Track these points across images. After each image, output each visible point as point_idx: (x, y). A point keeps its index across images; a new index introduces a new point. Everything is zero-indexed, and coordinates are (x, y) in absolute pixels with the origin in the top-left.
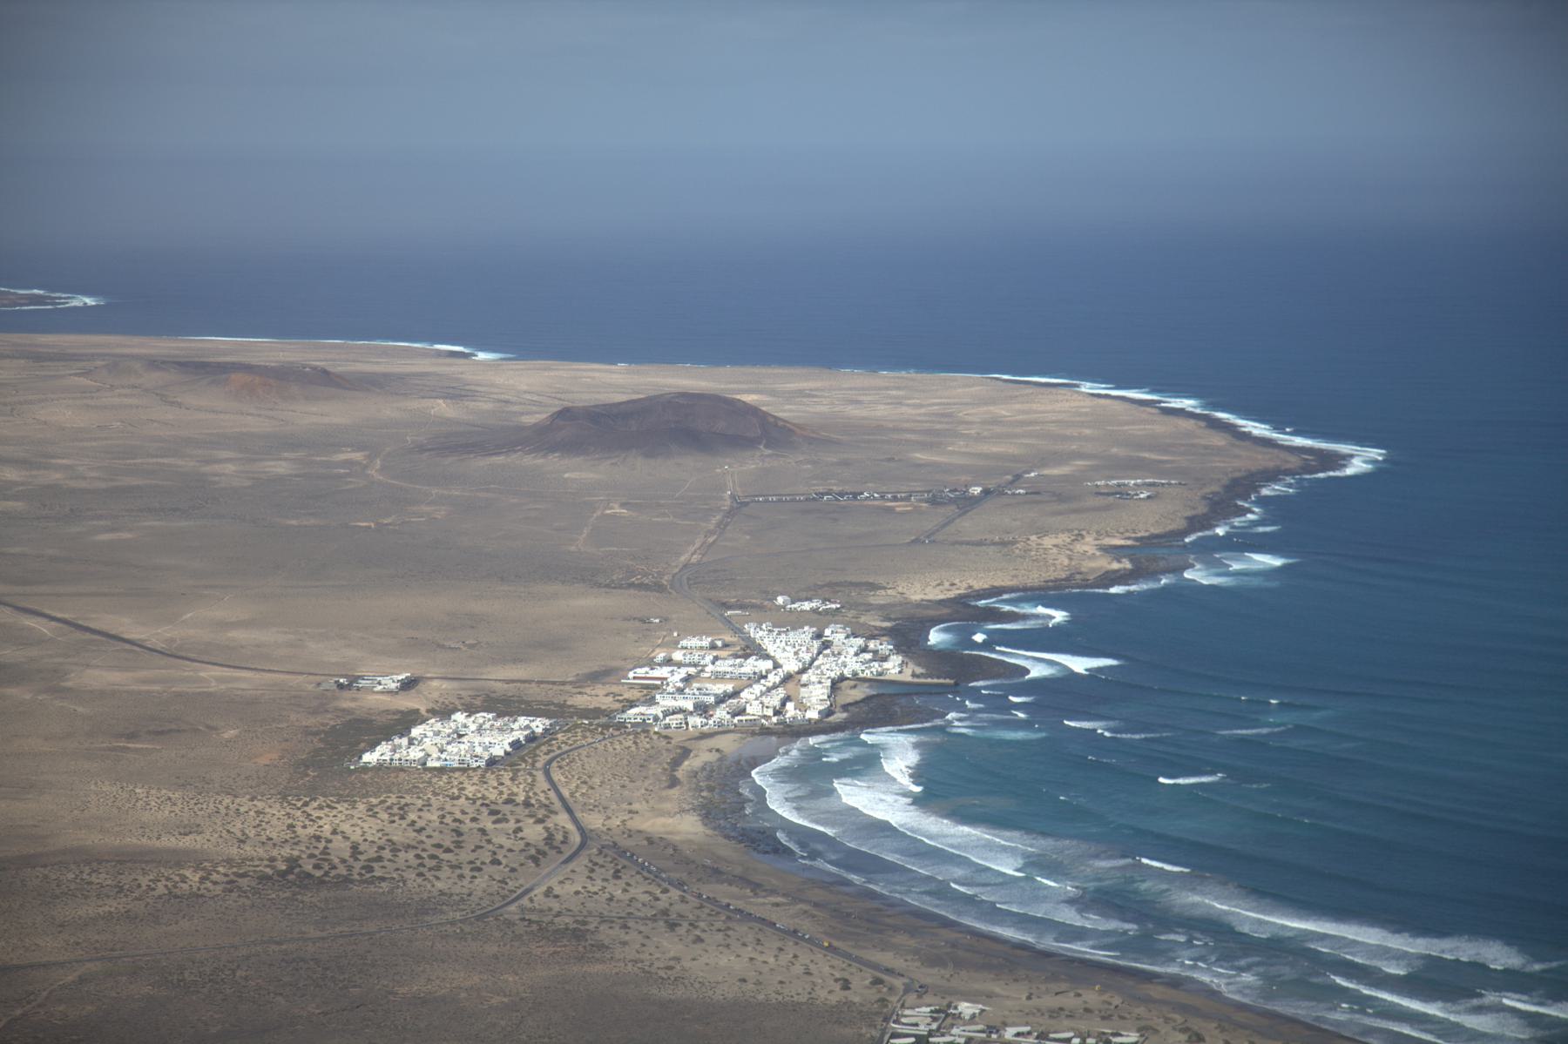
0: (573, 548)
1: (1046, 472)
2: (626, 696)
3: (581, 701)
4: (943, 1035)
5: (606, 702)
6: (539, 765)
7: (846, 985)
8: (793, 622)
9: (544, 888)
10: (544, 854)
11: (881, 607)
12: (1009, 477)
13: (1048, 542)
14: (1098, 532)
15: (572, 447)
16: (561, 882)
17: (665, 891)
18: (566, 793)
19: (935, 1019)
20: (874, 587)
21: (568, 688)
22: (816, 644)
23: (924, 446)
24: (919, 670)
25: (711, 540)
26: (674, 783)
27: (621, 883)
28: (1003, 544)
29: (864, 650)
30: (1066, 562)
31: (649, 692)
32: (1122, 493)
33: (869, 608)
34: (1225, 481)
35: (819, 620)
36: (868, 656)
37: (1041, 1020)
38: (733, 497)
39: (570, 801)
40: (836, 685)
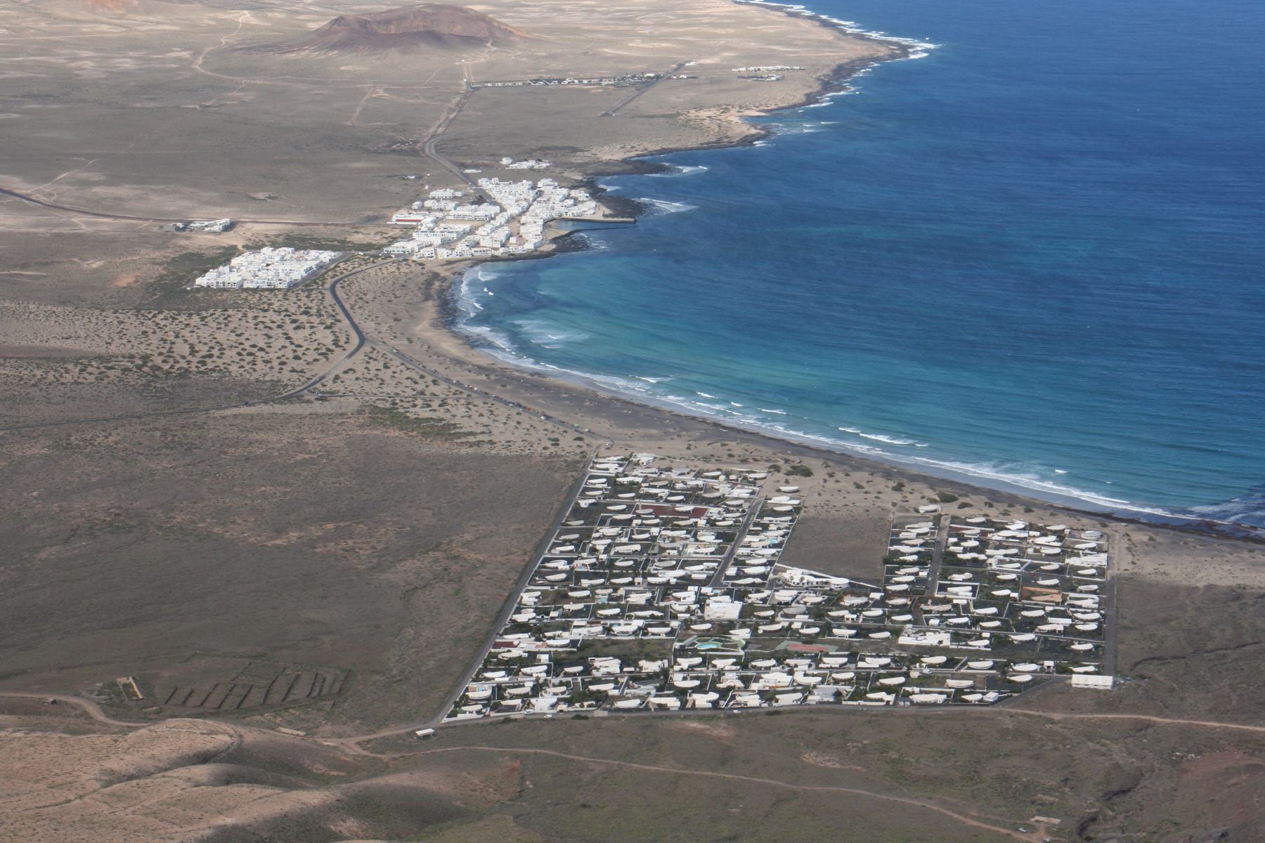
0: (349, 123)
1: (702, 61)
2: (391, 234)
3: (358, 238)
4: (626, 476)
5: (377, 239)
7: (556, 442)
9: (333, 376)
10: (332, 351)
13: (704, 114)
14: (741, 107)
16: (345, 372)
17: (422, 377)
18: (347, 307)
19: (621, 465)
20: (574, 150)
21: (347, 228)
22: (532, 193)
23: (609, 43)
24: (608, 211)
25: (452, 116)
26: (428, 297)
27: (389, 372)
28: (671, 116)
29: (568, 197)
30: (717, 129)
31: (407, 232)
32: (758, 78)
33: (570, 166)
34: (834, 66)
35: (534, 175)
36: (571, 202)
37: (696, 463)
38: (468, 83)
39: (351, 312)
40: (547, 224)
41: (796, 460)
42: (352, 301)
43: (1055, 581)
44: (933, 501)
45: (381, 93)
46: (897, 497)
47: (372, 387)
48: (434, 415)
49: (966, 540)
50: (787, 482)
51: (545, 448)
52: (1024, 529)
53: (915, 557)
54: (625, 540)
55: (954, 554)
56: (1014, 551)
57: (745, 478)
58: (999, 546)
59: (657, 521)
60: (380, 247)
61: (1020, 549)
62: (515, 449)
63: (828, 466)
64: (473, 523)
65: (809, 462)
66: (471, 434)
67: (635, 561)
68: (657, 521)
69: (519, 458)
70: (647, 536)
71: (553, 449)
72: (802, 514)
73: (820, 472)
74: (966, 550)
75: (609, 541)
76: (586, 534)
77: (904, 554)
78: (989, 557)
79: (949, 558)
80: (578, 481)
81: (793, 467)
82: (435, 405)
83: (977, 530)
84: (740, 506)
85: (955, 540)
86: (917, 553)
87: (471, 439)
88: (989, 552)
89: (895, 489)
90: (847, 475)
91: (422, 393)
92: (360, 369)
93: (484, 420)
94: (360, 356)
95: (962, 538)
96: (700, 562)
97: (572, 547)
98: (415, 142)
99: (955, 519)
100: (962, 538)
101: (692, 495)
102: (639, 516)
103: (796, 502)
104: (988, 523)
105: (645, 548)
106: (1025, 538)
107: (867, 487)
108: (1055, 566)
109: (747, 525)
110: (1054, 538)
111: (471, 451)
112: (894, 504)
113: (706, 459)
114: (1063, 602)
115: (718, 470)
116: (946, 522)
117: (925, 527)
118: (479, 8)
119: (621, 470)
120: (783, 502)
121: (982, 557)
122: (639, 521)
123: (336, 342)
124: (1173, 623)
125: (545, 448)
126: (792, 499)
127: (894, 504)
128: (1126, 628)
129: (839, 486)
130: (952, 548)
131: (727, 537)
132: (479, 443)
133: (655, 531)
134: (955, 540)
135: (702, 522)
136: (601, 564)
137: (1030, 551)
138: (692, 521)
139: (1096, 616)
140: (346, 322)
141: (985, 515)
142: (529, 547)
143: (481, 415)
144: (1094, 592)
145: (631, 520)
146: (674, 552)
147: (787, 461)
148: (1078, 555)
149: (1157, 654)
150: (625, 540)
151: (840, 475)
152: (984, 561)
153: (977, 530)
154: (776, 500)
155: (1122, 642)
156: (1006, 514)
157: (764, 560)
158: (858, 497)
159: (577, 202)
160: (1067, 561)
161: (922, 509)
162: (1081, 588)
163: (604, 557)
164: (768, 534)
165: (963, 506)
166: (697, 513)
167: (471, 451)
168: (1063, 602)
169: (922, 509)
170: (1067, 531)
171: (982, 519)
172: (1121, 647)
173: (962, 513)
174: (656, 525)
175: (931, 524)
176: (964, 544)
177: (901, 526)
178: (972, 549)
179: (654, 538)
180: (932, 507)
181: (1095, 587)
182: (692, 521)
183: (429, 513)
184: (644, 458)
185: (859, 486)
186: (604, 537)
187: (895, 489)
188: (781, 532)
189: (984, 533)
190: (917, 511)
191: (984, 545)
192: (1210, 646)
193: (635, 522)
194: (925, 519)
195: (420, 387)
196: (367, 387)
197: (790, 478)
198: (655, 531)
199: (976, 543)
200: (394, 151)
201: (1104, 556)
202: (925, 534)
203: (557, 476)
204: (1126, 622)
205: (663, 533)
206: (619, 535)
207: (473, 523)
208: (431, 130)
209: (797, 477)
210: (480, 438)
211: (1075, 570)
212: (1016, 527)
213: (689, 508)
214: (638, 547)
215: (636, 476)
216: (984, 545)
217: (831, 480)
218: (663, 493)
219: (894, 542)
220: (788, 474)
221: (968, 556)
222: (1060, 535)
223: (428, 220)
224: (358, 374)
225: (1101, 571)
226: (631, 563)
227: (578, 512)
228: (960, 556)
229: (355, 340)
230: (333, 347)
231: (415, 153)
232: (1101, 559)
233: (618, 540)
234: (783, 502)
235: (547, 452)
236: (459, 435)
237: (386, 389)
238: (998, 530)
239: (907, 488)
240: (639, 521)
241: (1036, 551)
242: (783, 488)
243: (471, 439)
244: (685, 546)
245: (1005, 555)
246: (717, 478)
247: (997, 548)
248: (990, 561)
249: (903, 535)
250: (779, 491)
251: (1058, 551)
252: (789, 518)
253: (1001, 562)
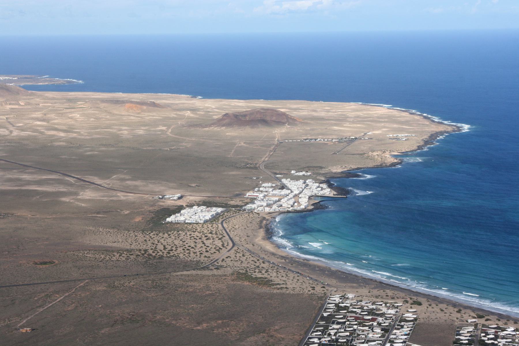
0: (229, 156)
1: (374, 132)
3: (232, 203)
4: (343, 303)
5: (240, 203)
6: (220, 222)
7: (313, 288)
8: (297, 178)
9: (221, 259)
11: (323, 174)
12: (363, 134)
13: (375, 154)
14: (390, 151)
15: (229, 125)
16: (227, 258)
17: (258, 260)
18: (228, 231)
19: (341, 299)
20: (321, 168)
21: (228, 199)
22: (304, 185)
23: (336, 125)
24: (335, 193)
25: (271, 153)
26: (261, 227)
27: (245, 258)
28: (361, 154)
29: (319, 187)
30: (380, 160)
31: (252, 200)
32: (397, 139)
33: (320, 174)
35: (305, 178)
36: (320, 189)
37: (373, 299)
38: (278, 140)
39: (229, 233)
40: (310, 198)
42: (230, 228)
44: (474, 318)
45: (242, 144)
46: (459, 315)
47: (237, 264)
48: (263, 276)
49: (489, 335)
50: (411, 308)
51: (309, 291)
52: (514, 331)
53: (467, 341)
54: (343, 330)
55: (484, 341)
56: (510, 340)
57: (393, 305)
58: (503, 338)
59: (356, 323)
60: (241, 206)
61: (512, 339)
62: (297, 291)
63: (428, 301)
64: (279, 322)
65: (420, 299)
66: (278, 284)
67: (347, 339)
68: (356, 323)
69: (298, 295)
70: (352, 329)
71: (312, 291)
72: (418, 321)
73: (425, 304)
74: (489, 339)
75: (336, 331)
76: (326, 328)
77: (462, 340)
78: (499, 342)
79: (482, 342)
80: (323, 305)
81: (414, 301)
82: (263, 272)
83: (494, 331)
84: (391, 317)
85: (484, 334)
86: (468, 340)
87: (278, 286)
89: (457, 312)
90: (437, 305)
91: (258, 267)
92: (233, 256)
93: (284, 279)
94: (233, 251)
96: (374, 341)
97: (320, 333)
98: (256, 164)
99: (484, 326)
100: (487, 334)
101: (371, 312)
102: (348, 321)
103: (415, 316)
104: (498, 328)
105: (351, 334)
106: (514, 335)
107: (446, 311)
109: (394, 325)
111: (278, 291)
112: (457, 318)
113: (377, 297)
115: (382, 302)
116: (480, 327)
117: (471, 329)
118: (282, 110)
119: (341, 300)
120: (410, 316)
121: (496, 342)
122: (348, 323)
123: (223, 245)
125: (309, 291)
126: (413, 315)
127: (457, 318)
129: (433, 310)
130: (483, 338)
131: (386, 330)
132: (282, 288)
133: (355, 327)
134: (484, 334)
135: (375, 324)
136: (333, 340)
138: (371, 323)
140: (227, 237)
141: (497, 324)
142: (302, 332)
143: (282, 276)
145: (345, 322)
146: (364, 336)
147: (411, 299)
150: (343, 330)
151: (434, 305)
152: (497, 344)
154: (407, 315)
156: (506, 324)
157: (402, 341)
158: (441, 315)
159: (322, 189)
161: (470, 321)
163: (334, 337)
164: (404, 329)
165: (487, 320)
166: (373, 320)
167: (278, 291)
169: (470, 321)
171: (495, 326)
173: (487, 323)
174: (356, 325)
175: (473, 327)
176: (488, 336)
177: (460, 328)
178: (491, 339)
179: (355, 330)
180: (474, 320)
182: (371, 323)
183: (261, 317)
184: (350, 296)
185: (442, 310)
186: (334, 329)
187: (457, 312)
188: (409, 329)
189: (496, 332)
190: (467, 322)
191: (496, 337)
193: (347, 323)
194: (471, 325)
195: (257, 264)
196: (236, 264)
197: (413, 306)
198: (355, 327)
199: (493, 336)
200: (247, 167)
202: (471, 332)
203: (314, 303)
205: (359, 328)
206: (340, 328)
207: (279, 322)
208: (263, 159)
209: (416, 306)
210: (282, 286)
212: (510, 330)
213: (370, 317)
214: (348, 334)
215: (347, 303)
216: (496, 337)
218: (359, 311)
219: (457, 335)
220: (412, 304)
221: (490, 342)
223: (261, 196)
224: (232, 259)
226: (345, 340)
227: (323, 318)
228: (486, 342)
229: (231, 244)
230: (222, 247)
231: (256, 168)
233: (340, 331)
234: (410, 316)
235: (310, 293)
236: (273, 285)
237: (243, 265)
239: (463, 312)
240: (348, 323)
242: (410, 310)
243: (278, 286)
244: (368, 334)
245: (506, 342)
246: (381, 305)
247: (502, 339)
248: (499, 344)
249: (461, 332)
250: (408, 311)
252: (412, 323)
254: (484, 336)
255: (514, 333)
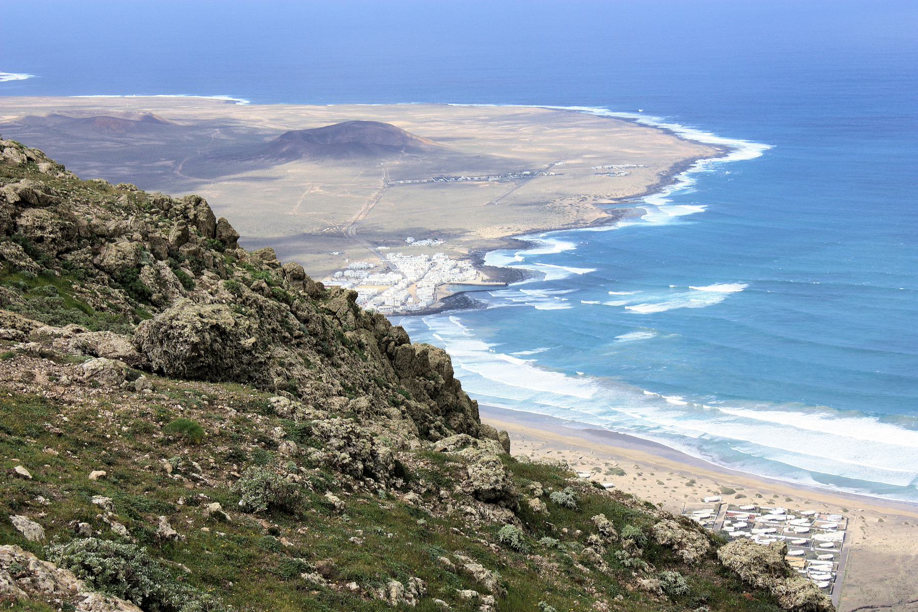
41: (613, 464)
43: (802, 552)
46: (689, 490)
49: (737, 522)
56: (774, 530)
58: (764, 526)
65: (623, 466)
74: (736, 530)
81: (611, 469)
83: (748, 514)
85: (729, 522)
88: (754, 531)
89: (688, 485)
95: (735, 521)
99: (731, 507)
100: (735, 521)
108: (803, 540)
110: (806, 520)
112: (686, 496)
114: (805, 568)
116: (724, 509)
121: (748, 534)
124: (887, 582)
127: (686, 496)
128: (850, 585)
129: (644, 483)
130: (726, 528)
137: (786, 530)
139: (829, 576)
144: (831, 560)
147: (607, 464)
148: (823, 533)
149: (870, 604)
153: (748, 514)
155: (846, 595)
156: (771, 502)
160: (813, 537)
162: (820, 557)
165: (739, 497)
168: (805, 568)
169: (707, 499)
170: (816, 515)
171: (752, 507)
172: (844, 599)
173: (737, 503)
176: (735, 525)
178: (741, 529)
180: (716, 498)
181: (831, 556)
185: (660, 483)
187: (688, 485)
189: (750, 517)
190: (703, 501)
192: (913, 598)
197: (608, 477)
199: (745, 524)
201: (842, 533)
204: (851, 581)
211: (817, 544)
216: (750, 526)
217: (639, 479)
222: (811, 519)
225: (837, 545)
232: (839, 536)
238: (763, 514)
241: (790, 530)
247: (760, 528)
251: (807, 529)
253: (763, 538)
254: (729, 525)
255: (783, 517)
